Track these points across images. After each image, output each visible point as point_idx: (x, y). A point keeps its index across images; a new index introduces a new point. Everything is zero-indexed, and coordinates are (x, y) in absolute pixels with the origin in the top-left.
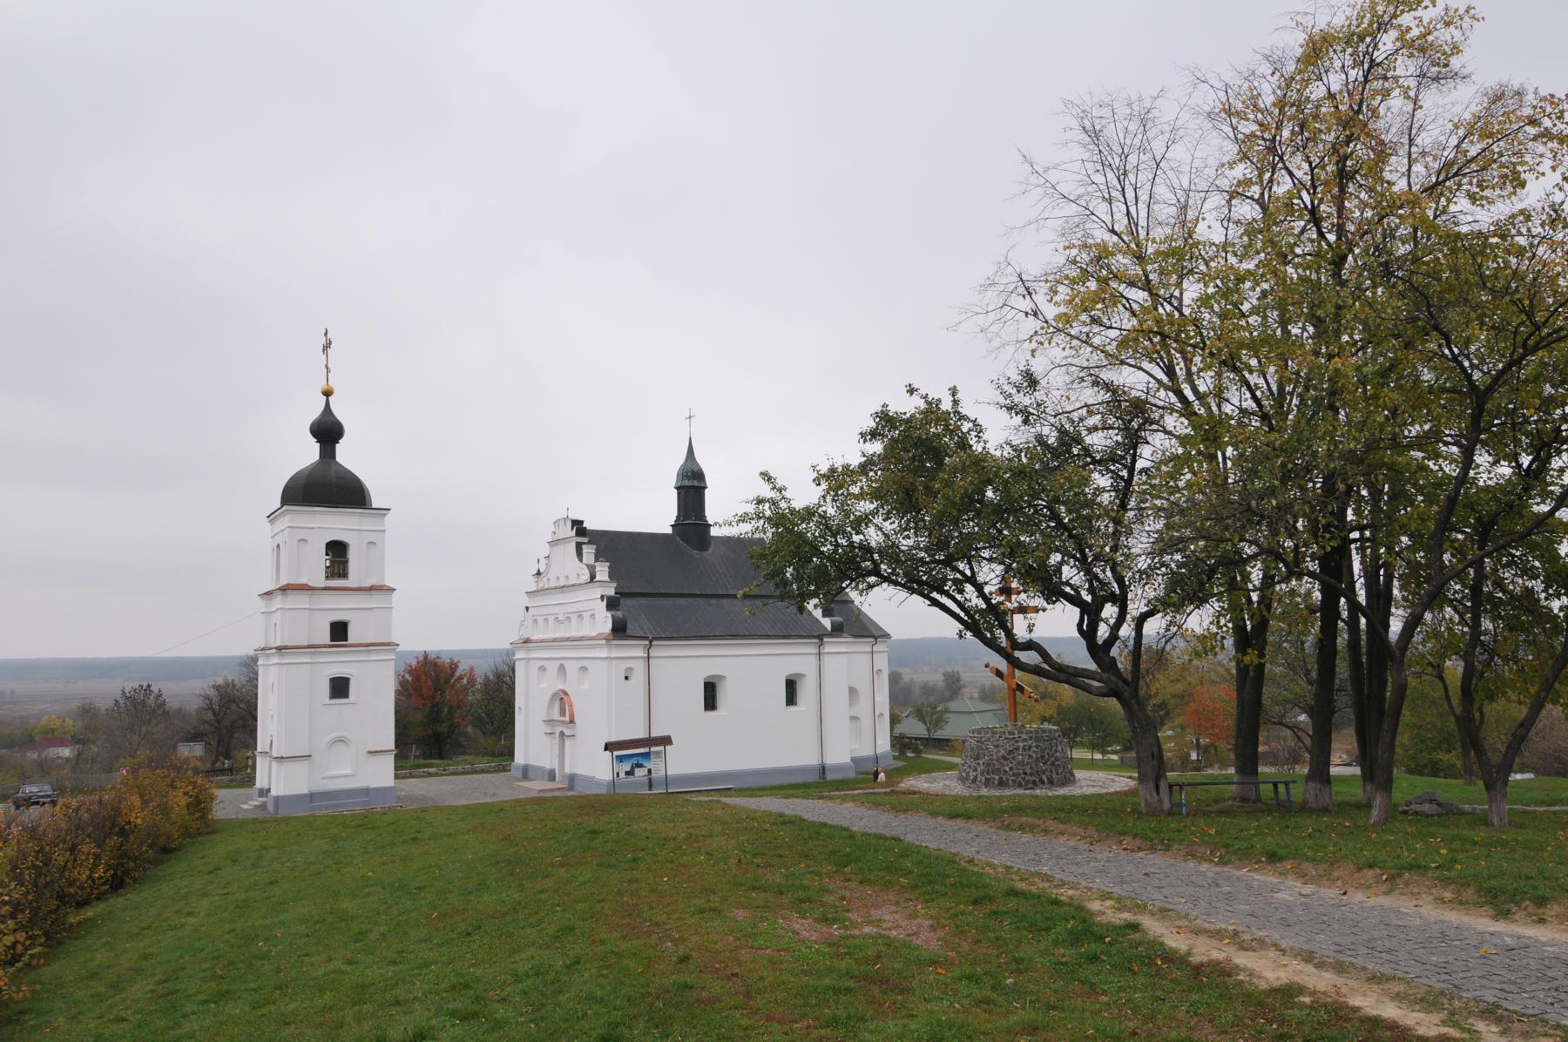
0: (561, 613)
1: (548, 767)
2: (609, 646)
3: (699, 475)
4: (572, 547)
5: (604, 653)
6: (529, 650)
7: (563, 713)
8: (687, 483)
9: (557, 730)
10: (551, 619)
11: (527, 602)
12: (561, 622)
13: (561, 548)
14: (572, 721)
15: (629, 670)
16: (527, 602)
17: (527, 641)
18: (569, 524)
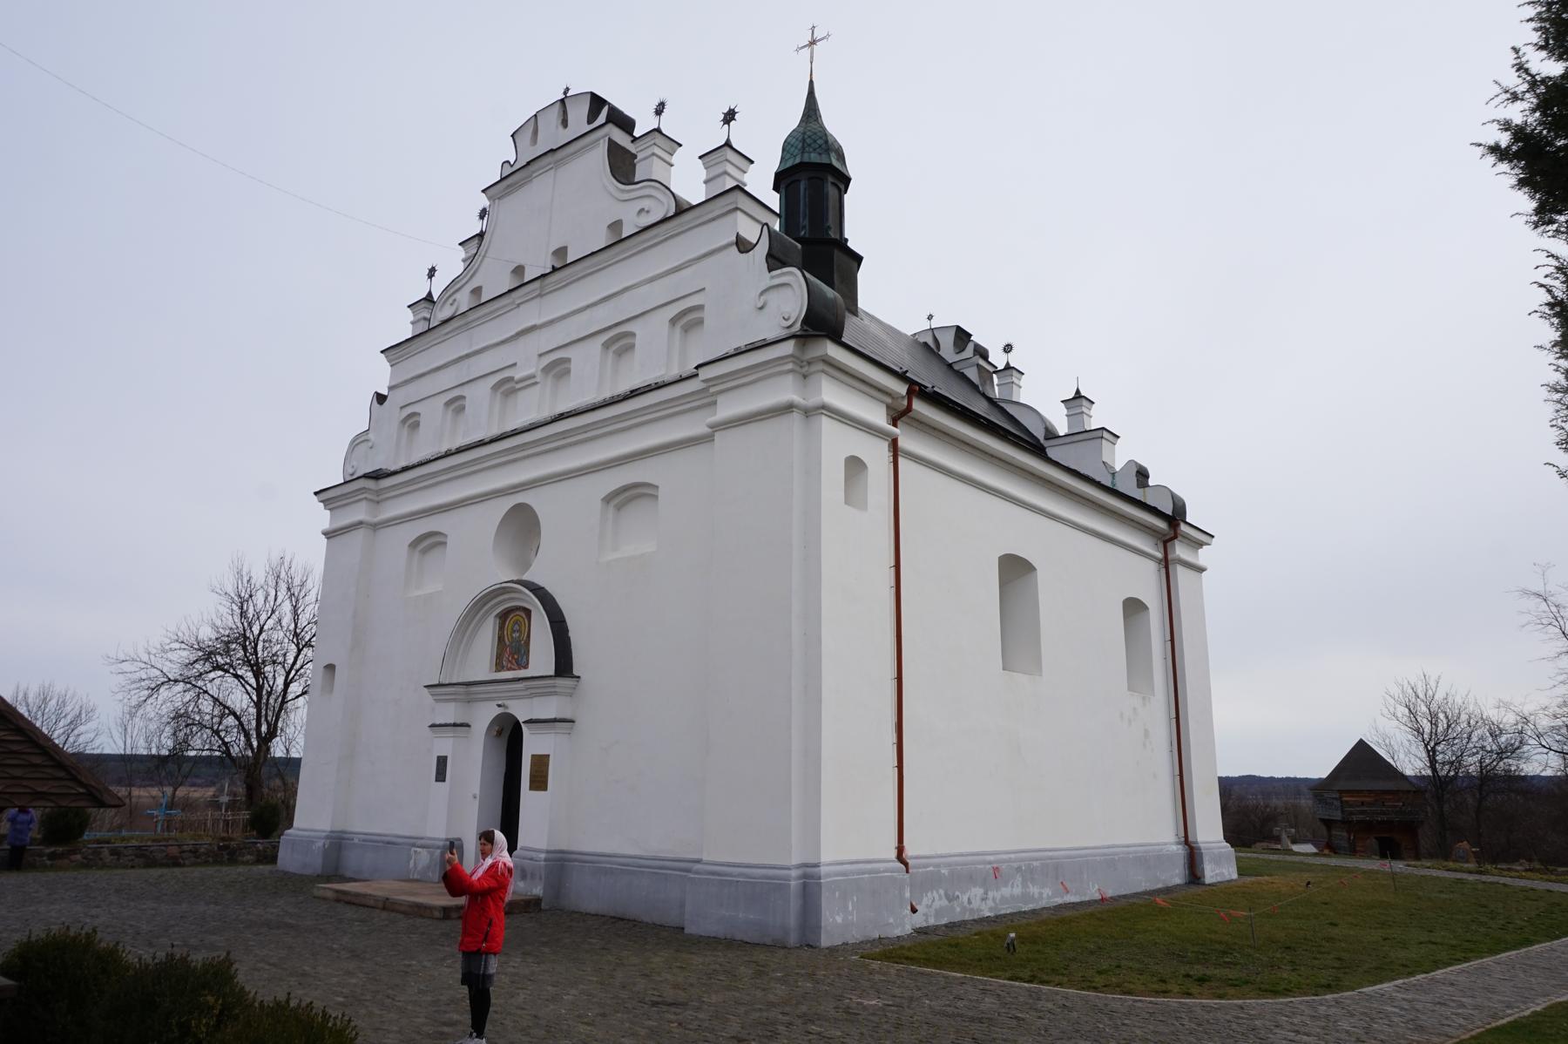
0: (526, 359)
1: (438, 831)
2: (803, 370)
3: (841, 157)
4: (596, 159)
5: (784, 390)
6: (378, 501)
7: (512, 651)
8: (814, 158)
9: (484, 715)
10: (479, 395)
11: (381, 376)
12: (529, 382)
13: (541, 187)
14: (564, 665)
15: (855, 465)
16: (381, 376)
17: (377, 475)
18: (579, 113)
